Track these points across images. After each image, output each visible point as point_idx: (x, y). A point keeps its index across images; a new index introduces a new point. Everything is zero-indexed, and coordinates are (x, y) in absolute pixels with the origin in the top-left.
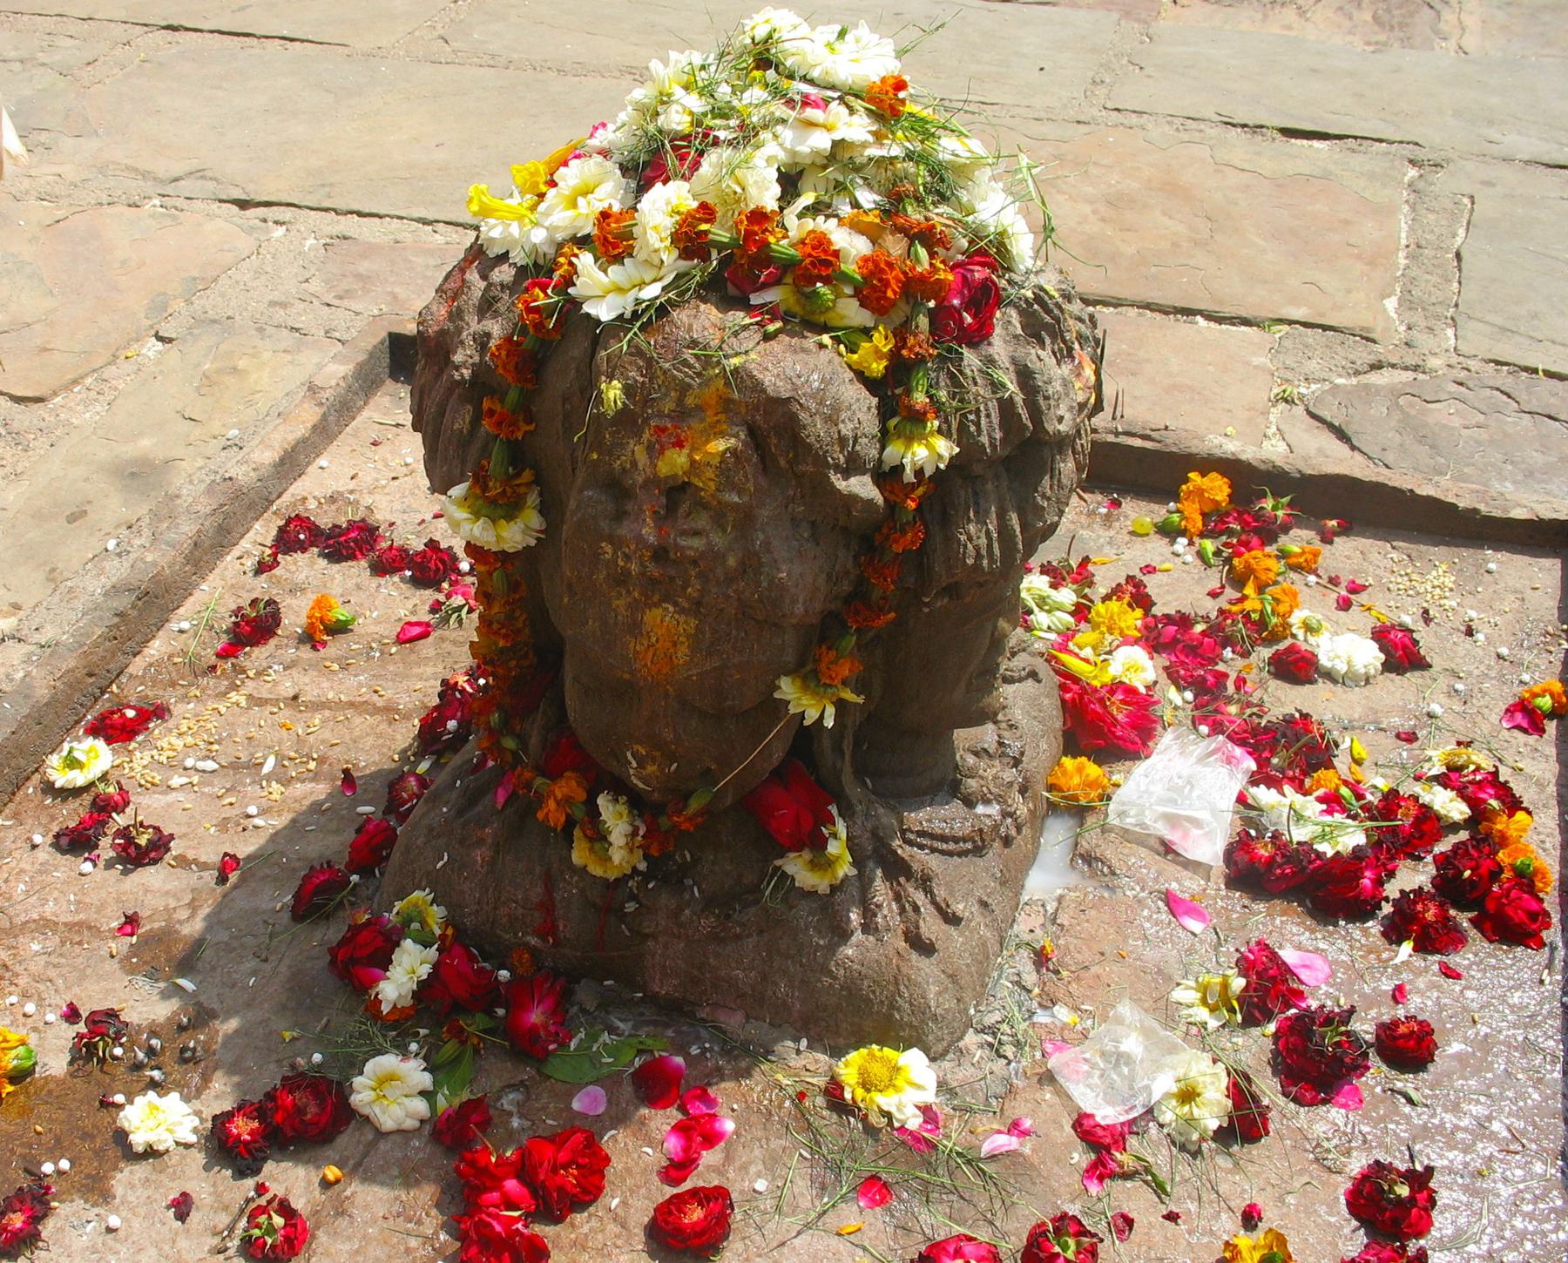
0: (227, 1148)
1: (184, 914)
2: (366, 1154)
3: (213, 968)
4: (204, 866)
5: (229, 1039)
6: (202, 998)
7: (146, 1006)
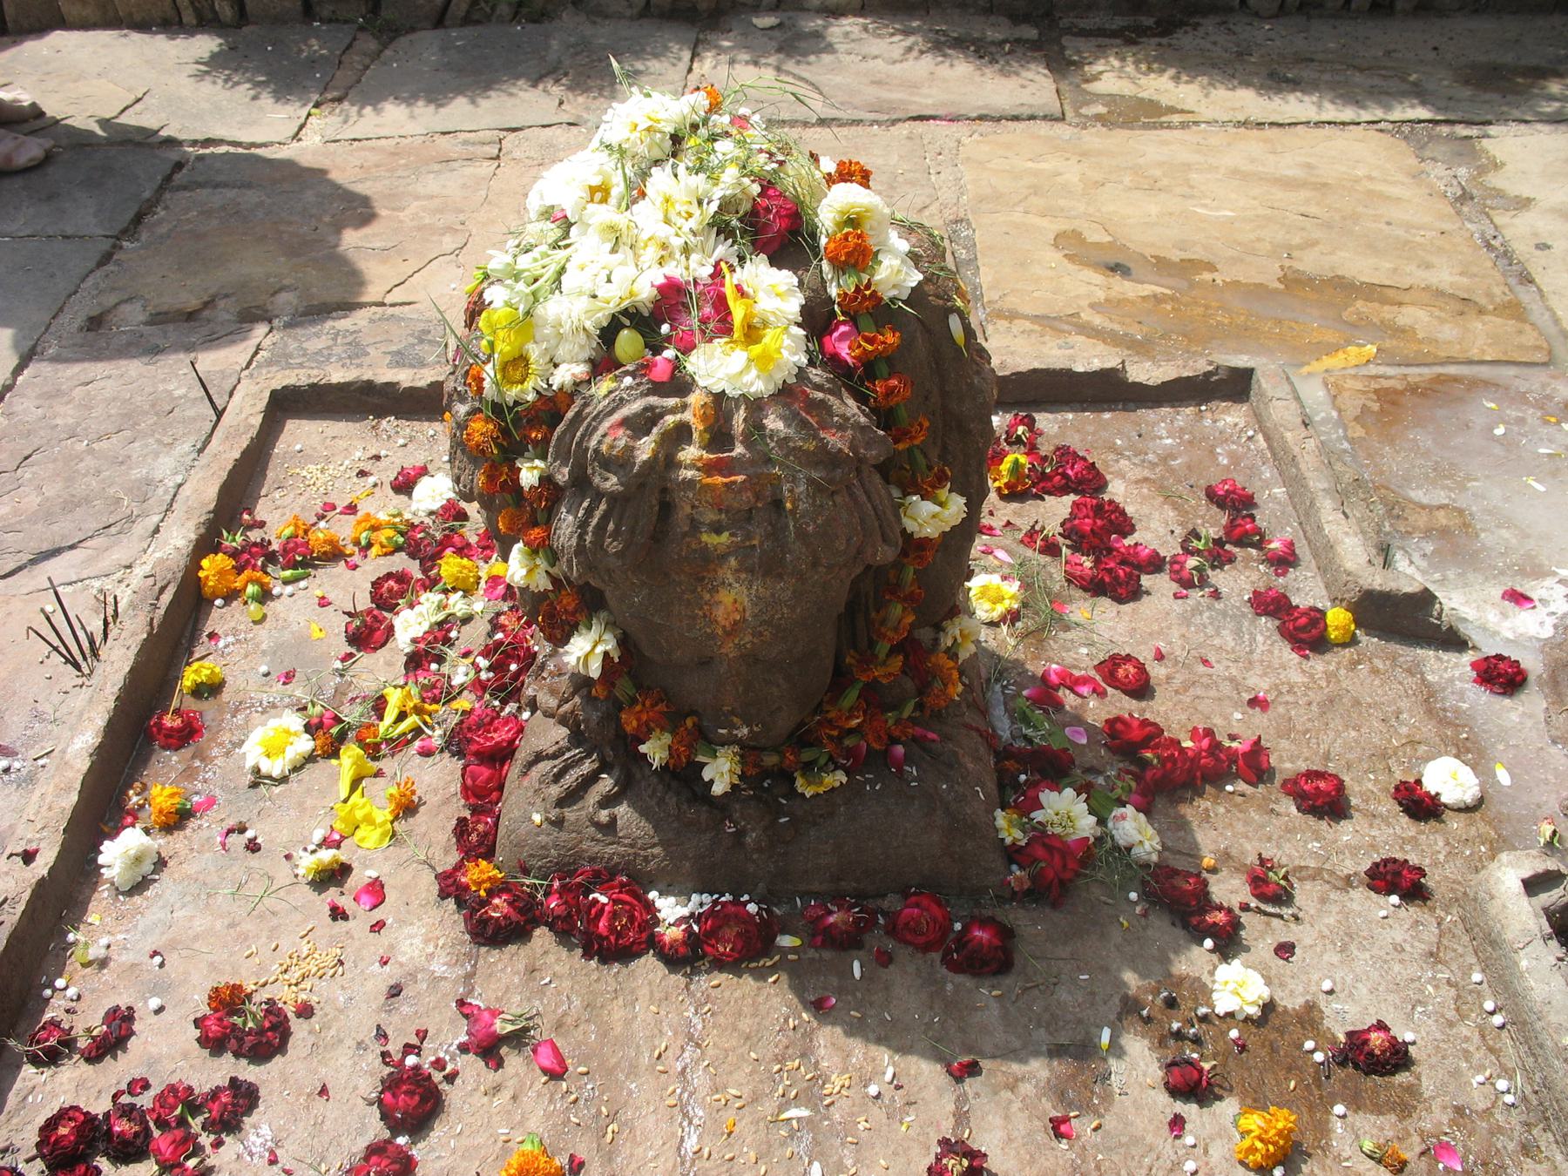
0: (1228, 943)
1: (1026, 1088)
2: (1180, 852)
3: (1080, 1021)
4: (961, 1100)
5: (1143, 976)
6: (1112, 1017)
7: (1137, 1065)
